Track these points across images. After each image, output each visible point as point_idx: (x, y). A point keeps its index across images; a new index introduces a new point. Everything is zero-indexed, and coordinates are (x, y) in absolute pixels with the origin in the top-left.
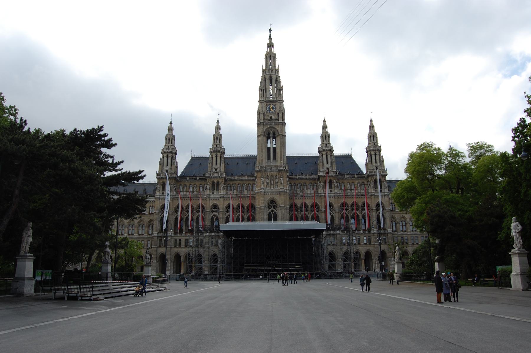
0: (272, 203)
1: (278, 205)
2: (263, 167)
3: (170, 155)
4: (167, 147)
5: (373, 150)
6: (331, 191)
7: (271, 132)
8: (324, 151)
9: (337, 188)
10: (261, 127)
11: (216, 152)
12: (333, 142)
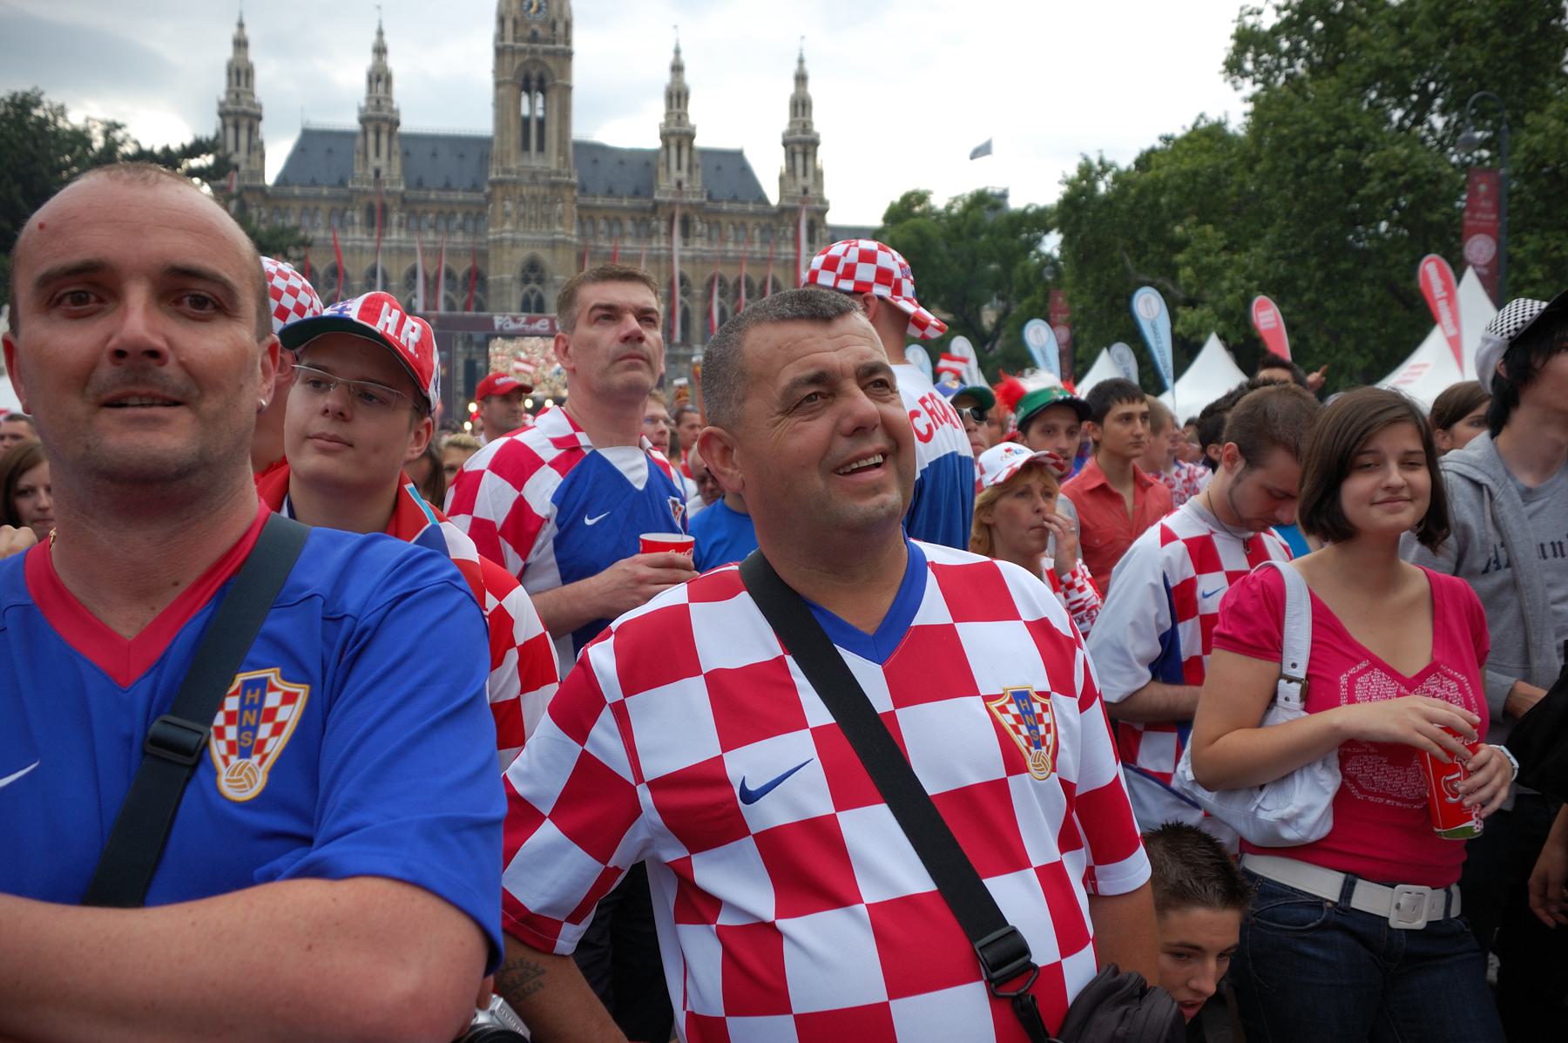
0: (533, 271)
1: (547, 276)
2: (508, 171)
3: (244, 123)
4: (233, 96)
5: (799, 142)
6: (686, 244)
7: (534, 73)
8: (672, 134)
9: (701, 235)
10: (508, 59)
11: (377, 119)
12: (697, 113)
